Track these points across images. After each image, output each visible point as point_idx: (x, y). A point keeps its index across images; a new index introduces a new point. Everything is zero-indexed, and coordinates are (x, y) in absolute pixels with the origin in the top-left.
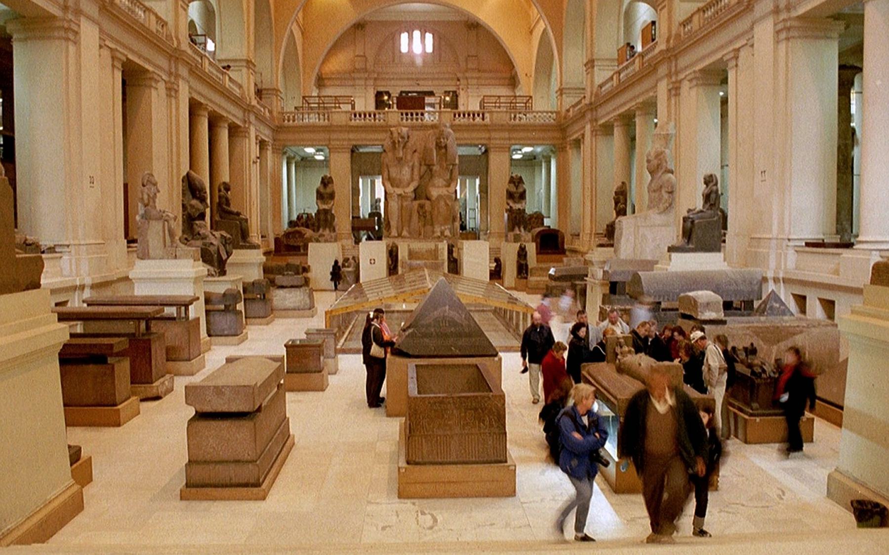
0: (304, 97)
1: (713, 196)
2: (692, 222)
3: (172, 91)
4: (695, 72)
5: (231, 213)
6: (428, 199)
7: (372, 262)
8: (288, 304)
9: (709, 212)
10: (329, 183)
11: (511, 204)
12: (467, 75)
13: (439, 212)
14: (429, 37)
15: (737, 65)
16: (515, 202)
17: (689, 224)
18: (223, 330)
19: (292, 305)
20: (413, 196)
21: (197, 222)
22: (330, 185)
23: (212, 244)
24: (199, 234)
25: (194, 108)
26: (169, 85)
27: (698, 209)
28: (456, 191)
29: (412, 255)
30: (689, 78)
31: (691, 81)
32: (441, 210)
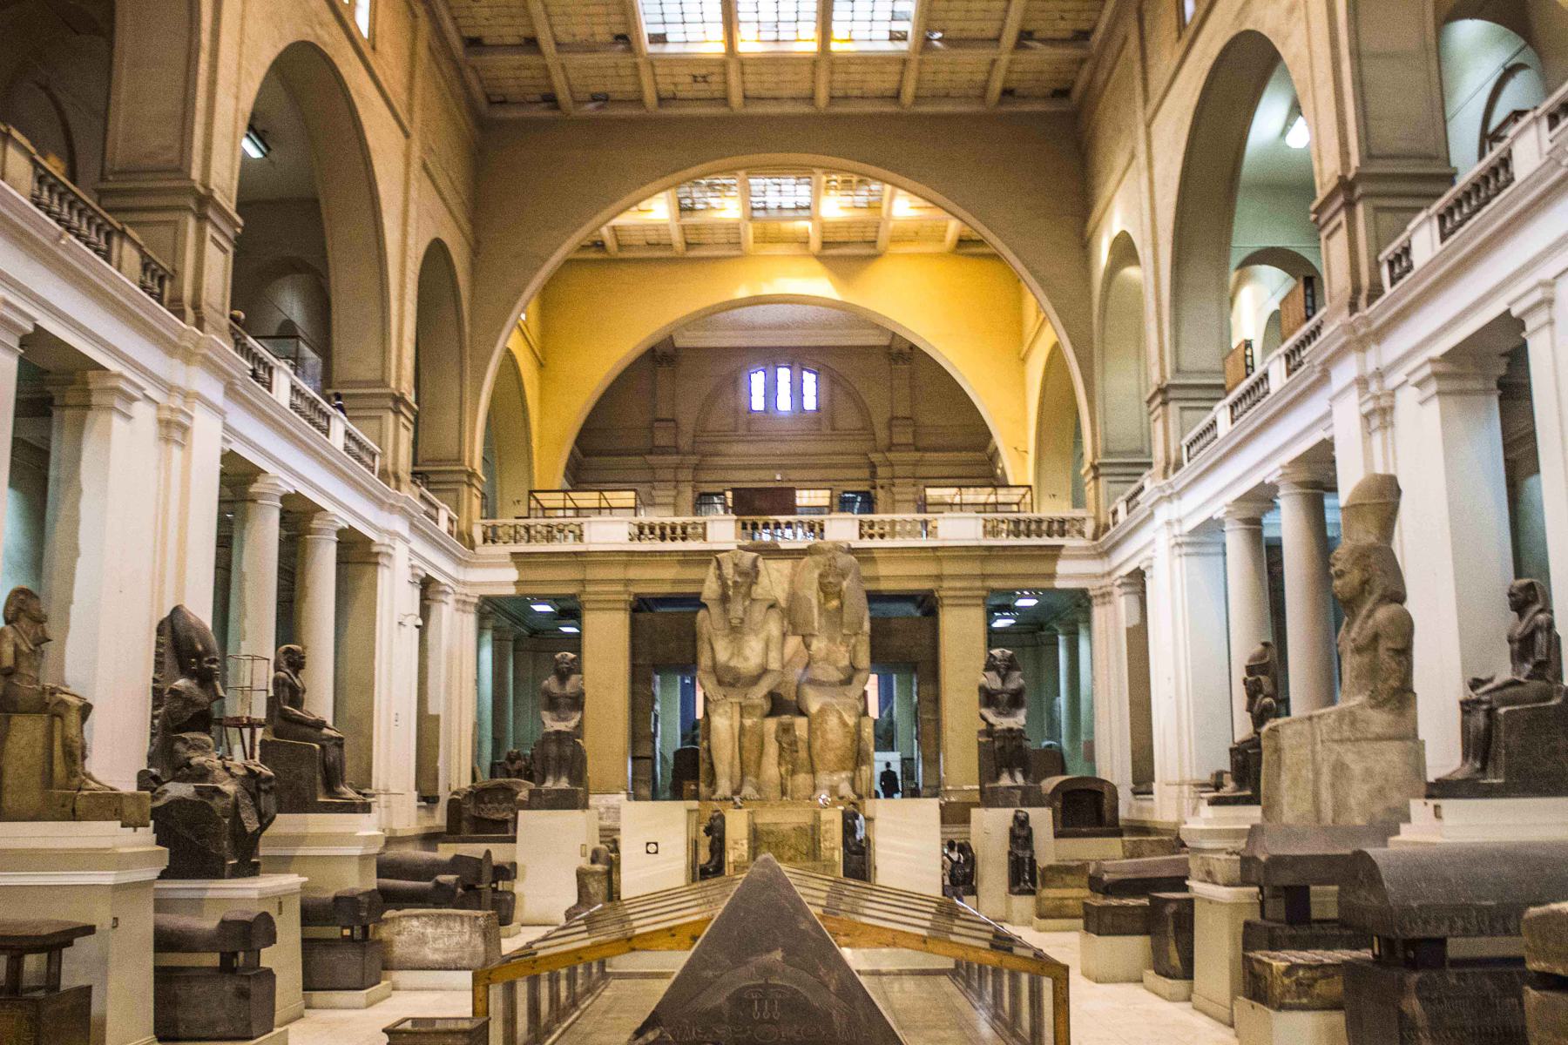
0: (531, 492)
1: (1541, 638)
2: (1490, 713)
3: (173, 430)
4: (1432, 361)
5: (301, 722)
6: (802, 713)
7: (652, 848)
8: (429, 953)
9: (1537, 684)
10: (571, 671)
11: (992, 719)
12: (891, 456)
13: (826, 742)
14: (809, 379)
15: (1551, 322)
16: (999, 714)
17: (1480, 720)
18: (212, 1024)
19: (438, 957)
20: (767, 706)
21: (187, 736)
22: (574, 678)
23: (217, 791)
24: (189, 766)
25: (238, 481)
26: (166, 415)
27: (1497, 681)
28: (865, 694)
29: (757, 838)
30: (1413, 380)
31: (1419, 385)
32: (830, 736)
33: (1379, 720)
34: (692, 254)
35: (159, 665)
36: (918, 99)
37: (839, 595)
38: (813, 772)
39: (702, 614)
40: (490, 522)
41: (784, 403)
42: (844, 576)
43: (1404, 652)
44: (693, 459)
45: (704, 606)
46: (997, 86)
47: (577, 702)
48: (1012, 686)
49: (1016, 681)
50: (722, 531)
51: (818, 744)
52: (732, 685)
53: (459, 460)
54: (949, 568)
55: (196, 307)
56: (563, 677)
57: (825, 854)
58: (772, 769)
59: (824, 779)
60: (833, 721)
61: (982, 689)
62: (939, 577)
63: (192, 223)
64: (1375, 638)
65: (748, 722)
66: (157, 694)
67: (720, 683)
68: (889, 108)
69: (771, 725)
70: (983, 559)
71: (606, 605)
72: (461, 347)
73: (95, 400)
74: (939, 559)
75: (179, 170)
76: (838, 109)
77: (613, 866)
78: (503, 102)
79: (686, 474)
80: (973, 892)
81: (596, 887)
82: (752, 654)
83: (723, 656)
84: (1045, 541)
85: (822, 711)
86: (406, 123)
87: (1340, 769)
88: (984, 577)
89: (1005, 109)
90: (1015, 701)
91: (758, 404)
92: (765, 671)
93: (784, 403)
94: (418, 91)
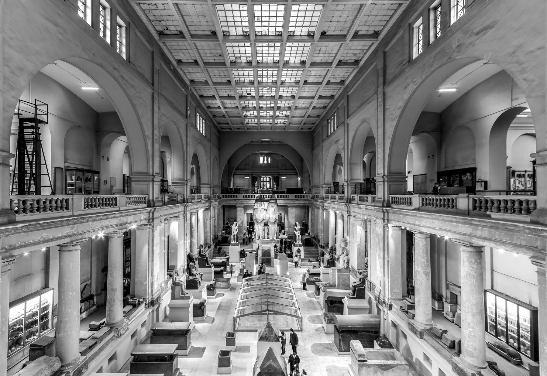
14: (269, 158)
41: (266, 162)
93: (266, 162)
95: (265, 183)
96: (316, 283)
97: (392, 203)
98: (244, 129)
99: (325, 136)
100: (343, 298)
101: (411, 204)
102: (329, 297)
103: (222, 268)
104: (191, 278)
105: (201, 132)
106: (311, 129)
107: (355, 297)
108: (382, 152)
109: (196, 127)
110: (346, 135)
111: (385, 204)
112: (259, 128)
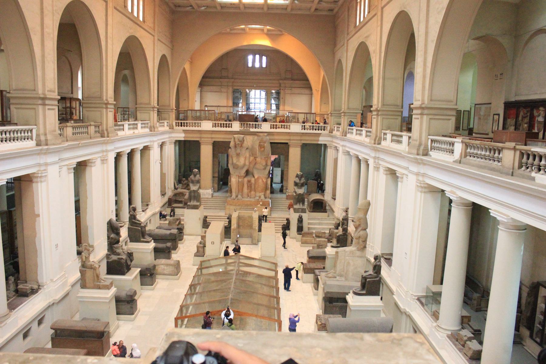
2: (366, 280)
5: (136, 223)
7: (213, 243)
8: (165, 272)
12: (285, 81)
14: (264, 58)
20: (244, 175)
22: (198, 176)
33: (358, 253)
34: (232, 32)
35: (108, 231)
36: (292, 9)
37: (264, 147)
38: (255, 191)
39: (230, 150)
40: (177, 121)
42: (265, 142)
43: (365, 241)
44: (233, 80)
45: (230, 148)
46: (313, 9)
47: (198, 182)
48: (302, 182)
49: (303, 180)
50: (236, 126)
51: (257, 186)
52: (237, 169)
53: (169, 106)
54: (292, 138)
55: (107, 130)
56: (195, 176)
57: (254, 227)
58: (246, 190)
59: (258, 194)
60: (260, 181)
61: (295, 182)
62: (290, 140)
63: (105, 110)
64: (360, 237)
65: (240, 180)
66: (108, 237)
67: (234, 168)
68: (284, 12)
69: (246, 180)
70: (301, 136)
71: (207, 144)
72: (169, 75)
73: (88, 164)
74: (290, 135)
75: (100, 98)
76: (269, 12)
77: (205, 246)
78: (179, 6)
79: (230, 84)
80: (289, 229)
81: (201, 249)
82: (241, 161)
83: (235, 161)
84: (317, 132)
85: (258, 178)
86: (153, 34)
87: (349, 263)
88: (301, 140)
89: (316, 13)
90: (302, 185)
91: (250, 65)
92: (245, 165)
94: (156, 23)
95: (257, 101)
96: (317, 271)
97: (431, 149)
98: (215, 7)
99: (352, 28)
100: (347, 294)
101: (452, 152)
102: (328, 293)
103: (169, 244)
104: (114, 257)
105: (135, 14)
106: (331, 10)
107: (364, 292)
108: (422, 64)
109: (126, 7)
110: (379, 28)
111: (421, 152)
112: (242, 7)
